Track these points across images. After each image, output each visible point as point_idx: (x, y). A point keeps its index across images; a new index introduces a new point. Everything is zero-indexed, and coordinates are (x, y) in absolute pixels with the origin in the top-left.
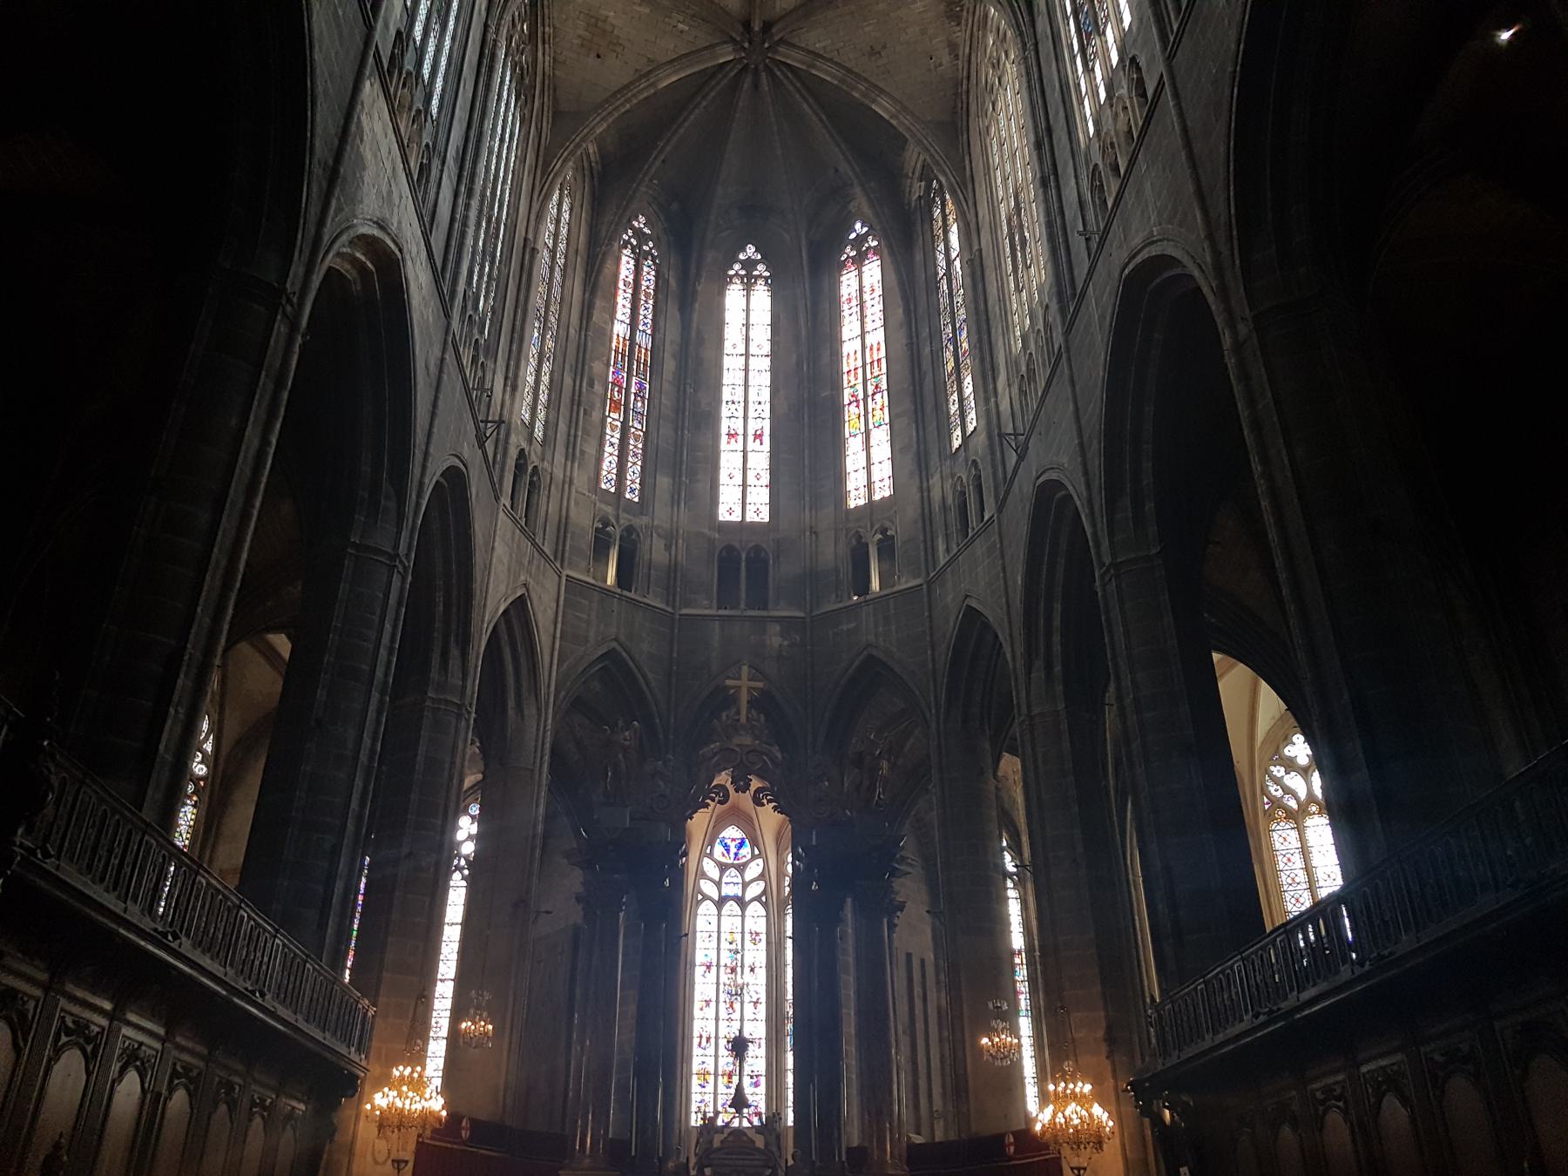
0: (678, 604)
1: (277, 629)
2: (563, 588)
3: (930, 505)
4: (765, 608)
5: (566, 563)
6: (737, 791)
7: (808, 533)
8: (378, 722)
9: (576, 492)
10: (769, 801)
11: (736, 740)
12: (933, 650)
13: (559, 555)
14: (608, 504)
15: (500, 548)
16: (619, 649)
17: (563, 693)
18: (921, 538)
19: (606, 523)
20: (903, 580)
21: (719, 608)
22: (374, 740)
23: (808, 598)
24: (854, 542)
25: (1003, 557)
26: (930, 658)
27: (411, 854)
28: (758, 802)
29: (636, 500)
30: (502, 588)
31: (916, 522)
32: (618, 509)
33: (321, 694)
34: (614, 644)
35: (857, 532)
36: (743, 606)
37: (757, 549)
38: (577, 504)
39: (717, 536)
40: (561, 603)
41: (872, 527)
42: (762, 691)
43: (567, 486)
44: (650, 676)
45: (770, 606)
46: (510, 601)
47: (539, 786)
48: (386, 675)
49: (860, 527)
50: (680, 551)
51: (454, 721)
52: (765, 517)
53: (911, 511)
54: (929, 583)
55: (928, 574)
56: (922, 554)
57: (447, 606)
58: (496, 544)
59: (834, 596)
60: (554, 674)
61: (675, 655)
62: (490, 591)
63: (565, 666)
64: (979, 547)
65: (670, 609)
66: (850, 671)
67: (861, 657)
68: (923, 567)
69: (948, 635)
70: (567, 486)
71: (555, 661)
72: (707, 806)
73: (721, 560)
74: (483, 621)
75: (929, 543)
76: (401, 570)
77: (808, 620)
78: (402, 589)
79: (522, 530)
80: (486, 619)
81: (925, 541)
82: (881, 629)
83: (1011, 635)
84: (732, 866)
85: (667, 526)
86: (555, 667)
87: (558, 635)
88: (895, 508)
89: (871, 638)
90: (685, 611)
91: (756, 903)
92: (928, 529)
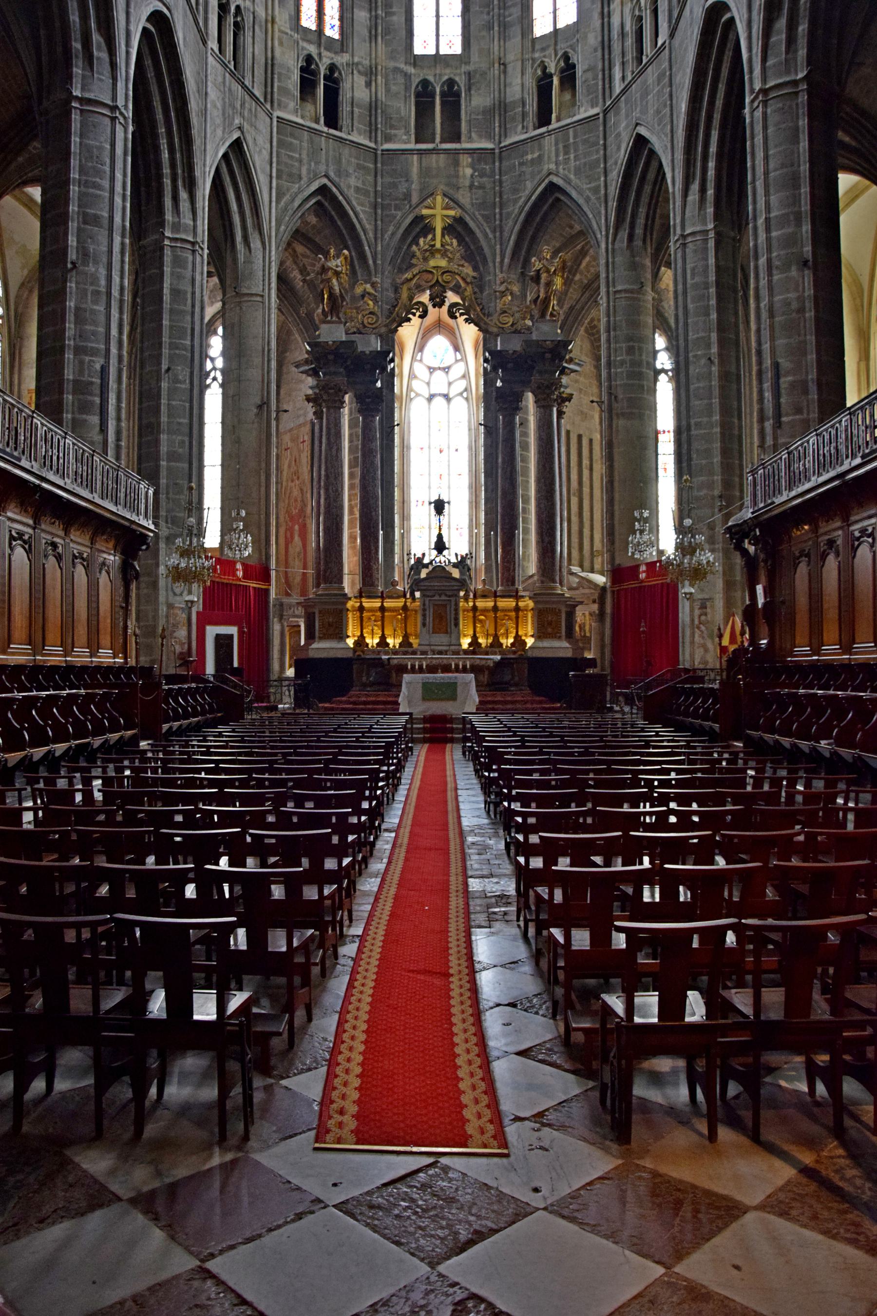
0: (379, 139)
1: (32, 182)
2: (275, 129)
3: (609, 31)
4: (457, 138)
5: (276, 104)
6: (434, 306)
7: (496, 65)
8: (123, 262)
9: (280, 31)
10: (461, 314)
11: (432, 263)
12: (606, 176)
13: (269, 96)
14: (309, 42)
15: (213, 94)
16: (329, 184)
17: (283, 228)
18: (600, 66)
19: (309, 59)
20: (582, 110)
21: (417, 141)
22: (122, 278)
23: (497, 129)
24: (539, 72)
25: (671, 85)
26: (602, 184)
27: (168, 370)
28: (452, 316)
29: (337, 36)
30: (219, 132)
31: (595, 50)
32: (319, 45)
33: (72, 241)
34: (325, 181)
35: (542, 62)
36: (438, 139)
37: (451, 83)
38: (281, 44)
39: (411, 70)
40: (275, 144)
41: (556, 55)
42: (454, 217)
43: (270, 25)
44: (358, 208)
45: (463, 138)
46: (227, 144)
47: (269, 309)
48: (123, 220)
49: (545, 56)
50: (379, 88)
51: (190, 258)
52: (457, 49)
53: (593, 39)
54: (606, 112)
55: (604, 101)
56: (600, 83)
57: (172, 151)
58: (209, 90)
59: (520, 127)
60: (273, 210)
61: (379, 188)
62: (208, 135)
63: (282, 203)
64: (651, 75)
65: (372, 145)
66: (533, 198)
67: (543, 185)
68: (600, 96)
69: (620, 162)
70: (270, 25)
71: (274, 199)
72: (409, 320)
73: (418, 95)
74: (204, 165)
75: (607, 72)
76: (122, 121)
77: (497, 151)
78: (126, 139)
79: (232, 74)
80: (208, 163)
81: (603, 70)
82: (561, 158)
83: (673, 161)
84: (439, 368)
85: (367, 62)
86: (274, 204)
87: (274, 174)
88: (578, 36)
89: (552, 166)
90: (387, 146)
91: (459, 398)
92: (606, 57)
